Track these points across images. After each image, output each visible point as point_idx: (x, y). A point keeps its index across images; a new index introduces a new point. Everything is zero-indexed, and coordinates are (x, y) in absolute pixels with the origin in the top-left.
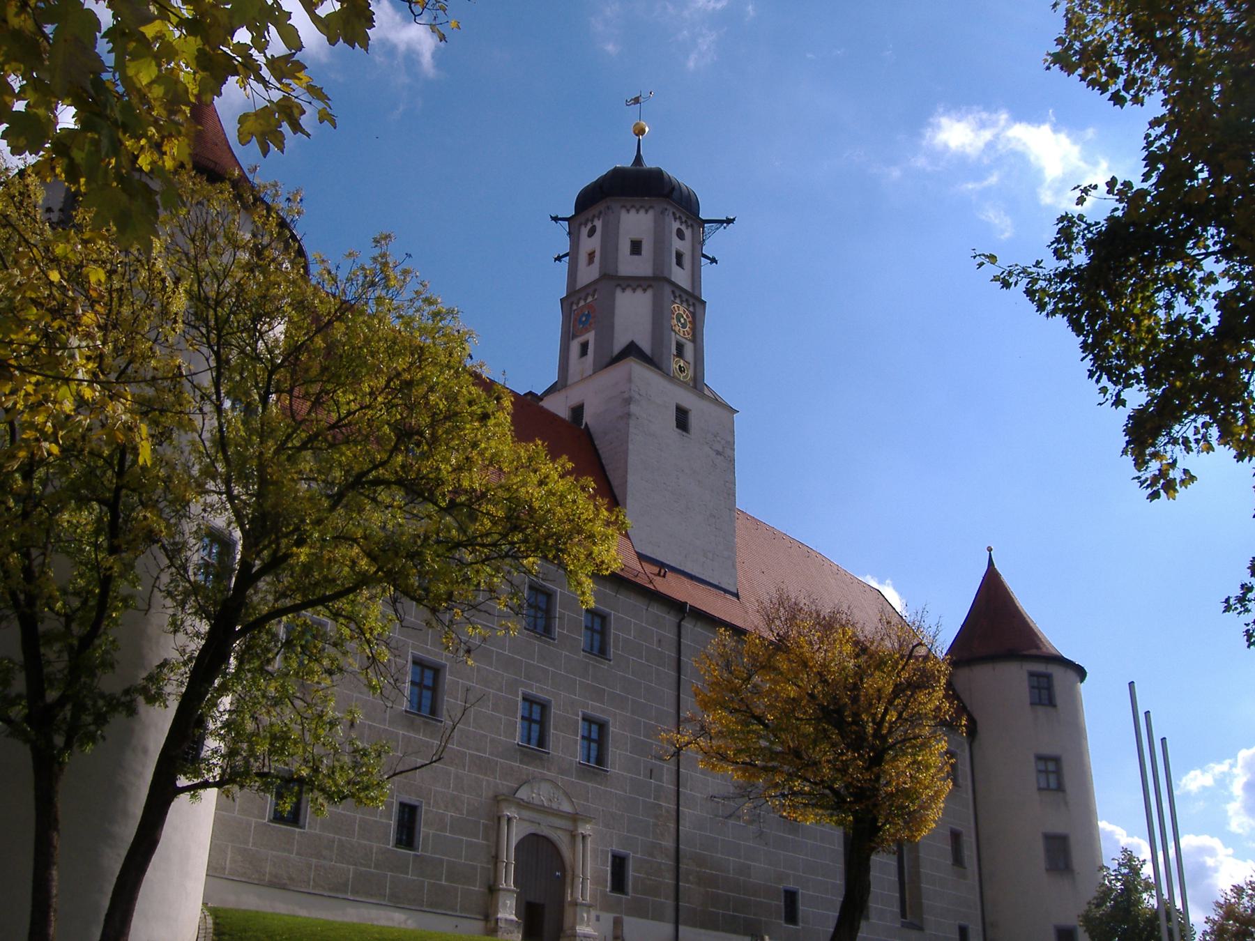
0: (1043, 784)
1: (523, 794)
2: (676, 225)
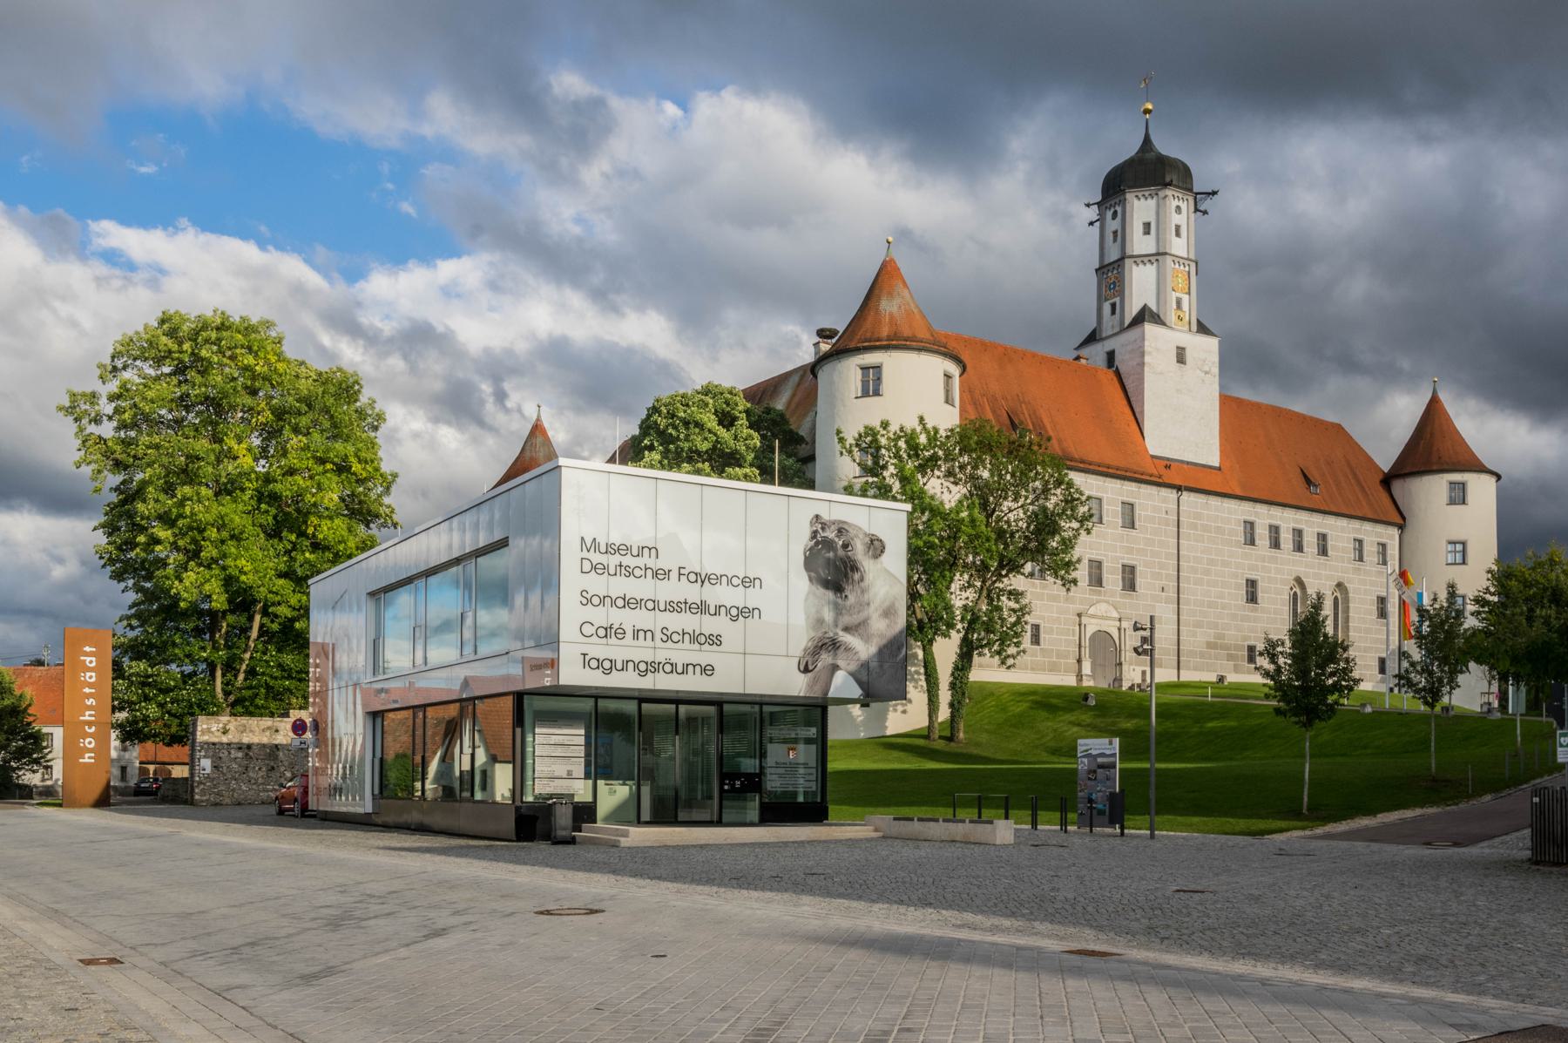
1: (1092, 611)
2: (1175, 203)
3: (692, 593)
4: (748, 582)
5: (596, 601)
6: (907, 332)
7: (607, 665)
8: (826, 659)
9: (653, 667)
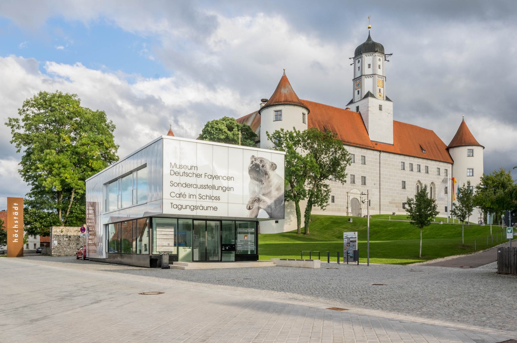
0: (468, 175)
2: (378, 58)
3: (210, 182)
4: (229, 178)
5: (176, 185)
6: (290, 100)
7: (180, 207)
8: (256, 205)
9: (196, 208)
